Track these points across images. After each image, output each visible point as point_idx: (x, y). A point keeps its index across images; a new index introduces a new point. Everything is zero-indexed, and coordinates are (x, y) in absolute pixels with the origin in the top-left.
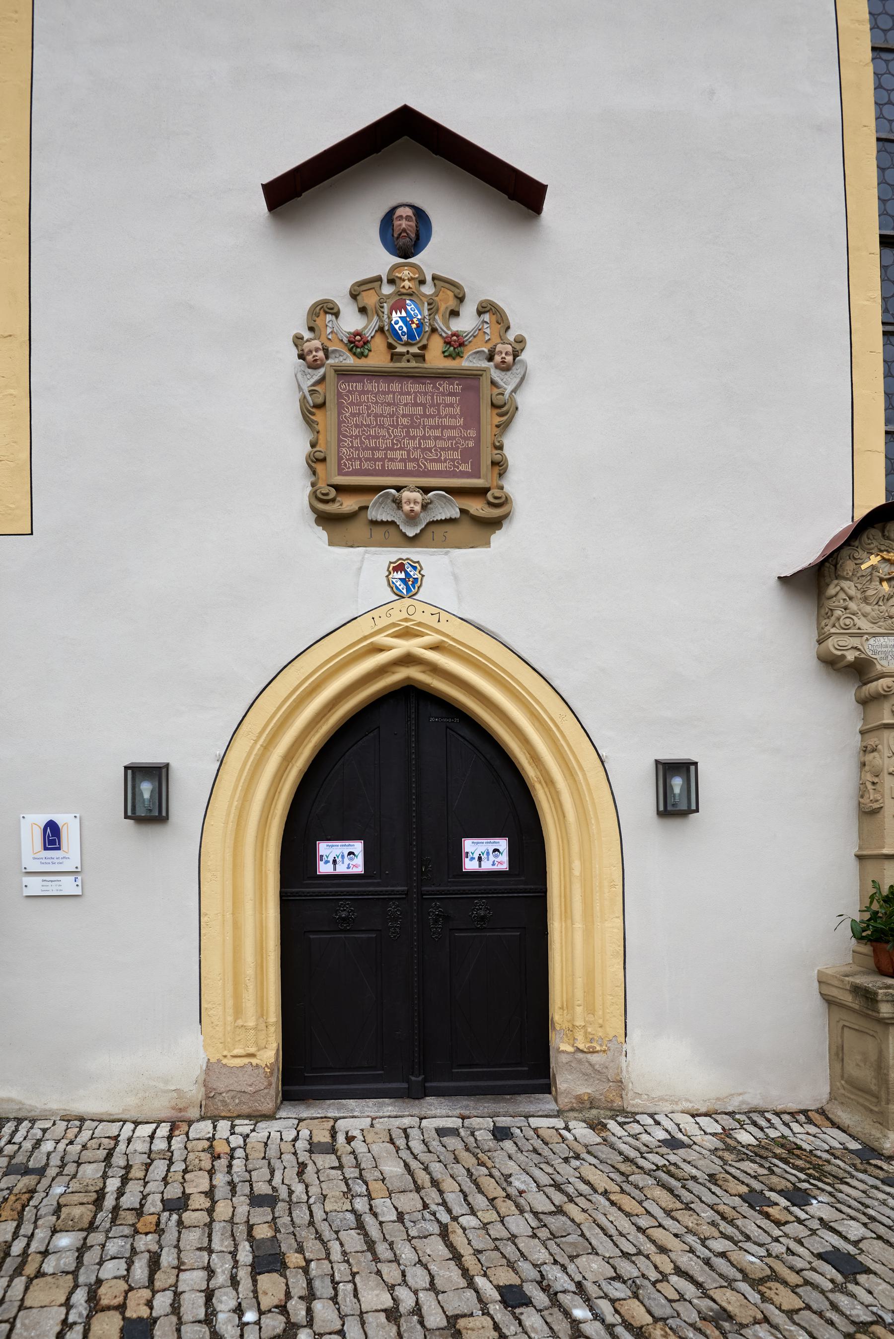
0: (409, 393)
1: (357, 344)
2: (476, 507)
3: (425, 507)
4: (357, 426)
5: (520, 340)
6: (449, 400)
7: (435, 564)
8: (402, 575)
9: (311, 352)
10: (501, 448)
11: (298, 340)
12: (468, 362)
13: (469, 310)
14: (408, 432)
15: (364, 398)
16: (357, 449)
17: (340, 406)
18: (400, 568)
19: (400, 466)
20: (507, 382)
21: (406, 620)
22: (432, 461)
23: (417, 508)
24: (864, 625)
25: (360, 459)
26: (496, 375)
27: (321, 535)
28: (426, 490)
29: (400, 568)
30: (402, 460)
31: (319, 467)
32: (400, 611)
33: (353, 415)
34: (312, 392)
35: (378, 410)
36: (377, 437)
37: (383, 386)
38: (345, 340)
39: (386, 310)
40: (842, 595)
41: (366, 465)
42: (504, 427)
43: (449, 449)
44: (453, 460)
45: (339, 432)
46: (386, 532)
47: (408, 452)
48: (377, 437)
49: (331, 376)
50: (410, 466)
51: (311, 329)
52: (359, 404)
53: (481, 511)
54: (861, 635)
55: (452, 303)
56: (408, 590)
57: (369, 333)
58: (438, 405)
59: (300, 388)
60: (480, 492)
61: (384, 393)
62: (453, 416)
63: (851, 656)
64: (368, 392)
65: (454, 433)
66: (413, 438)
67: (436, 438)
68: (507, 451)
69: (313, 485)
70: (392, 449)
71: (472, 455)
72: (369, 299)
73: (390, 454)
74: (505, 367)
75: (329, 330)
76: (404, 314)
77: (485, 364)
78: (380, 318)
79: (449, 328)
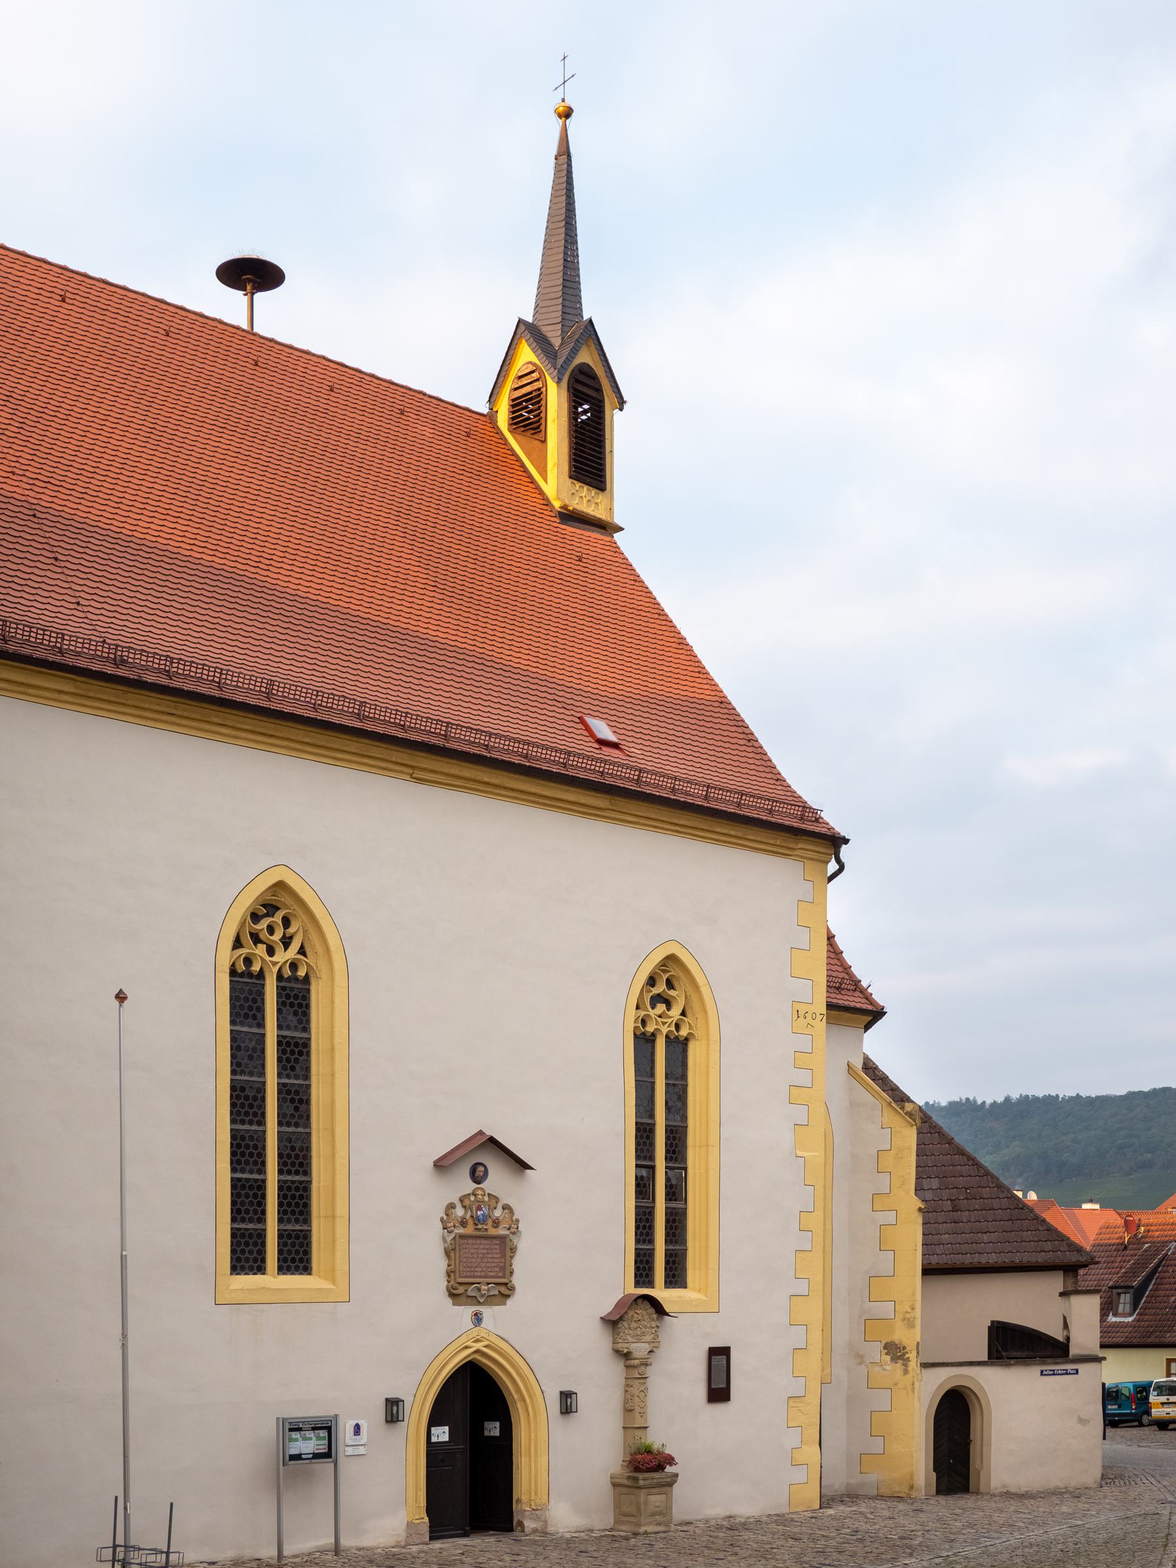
2: (503, 1289)
7: (487, 1312)
53: (504, 1292)
71: (503, 1269)
72: (467, 1202)
77: (507, 1232)
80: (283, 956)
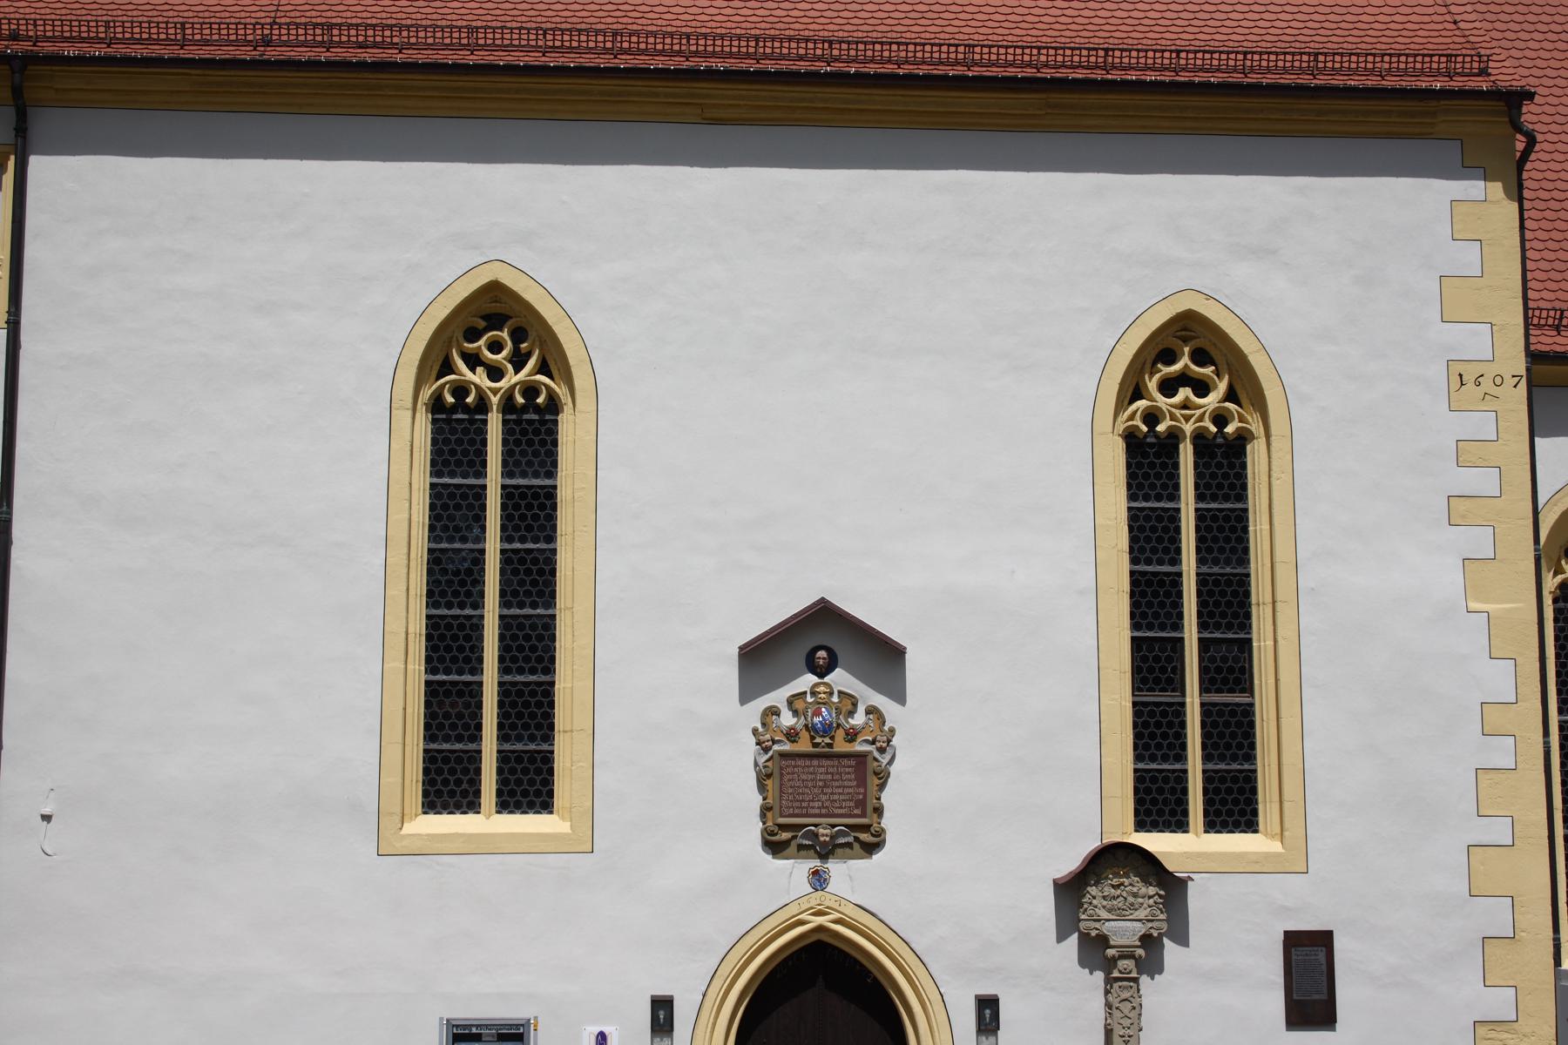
1: (792, 735)
2: (864, 837)
5: (892, 731)
7: (837, 869)
11: (755, 731)
12: (859, 747)
13: (861, 709)
18: (816, 873)
20: (884, 760)
24: (1104, 915)
26: (876, 754)
28: (833, 826)
32: (816, 899)
42: (882, 787)
49: (777, 757)
55: (850, 707)
60: (866, 828)
63: (1093, 933)
71: (862, 804)
72: (799, 705)
80: (511, 379)
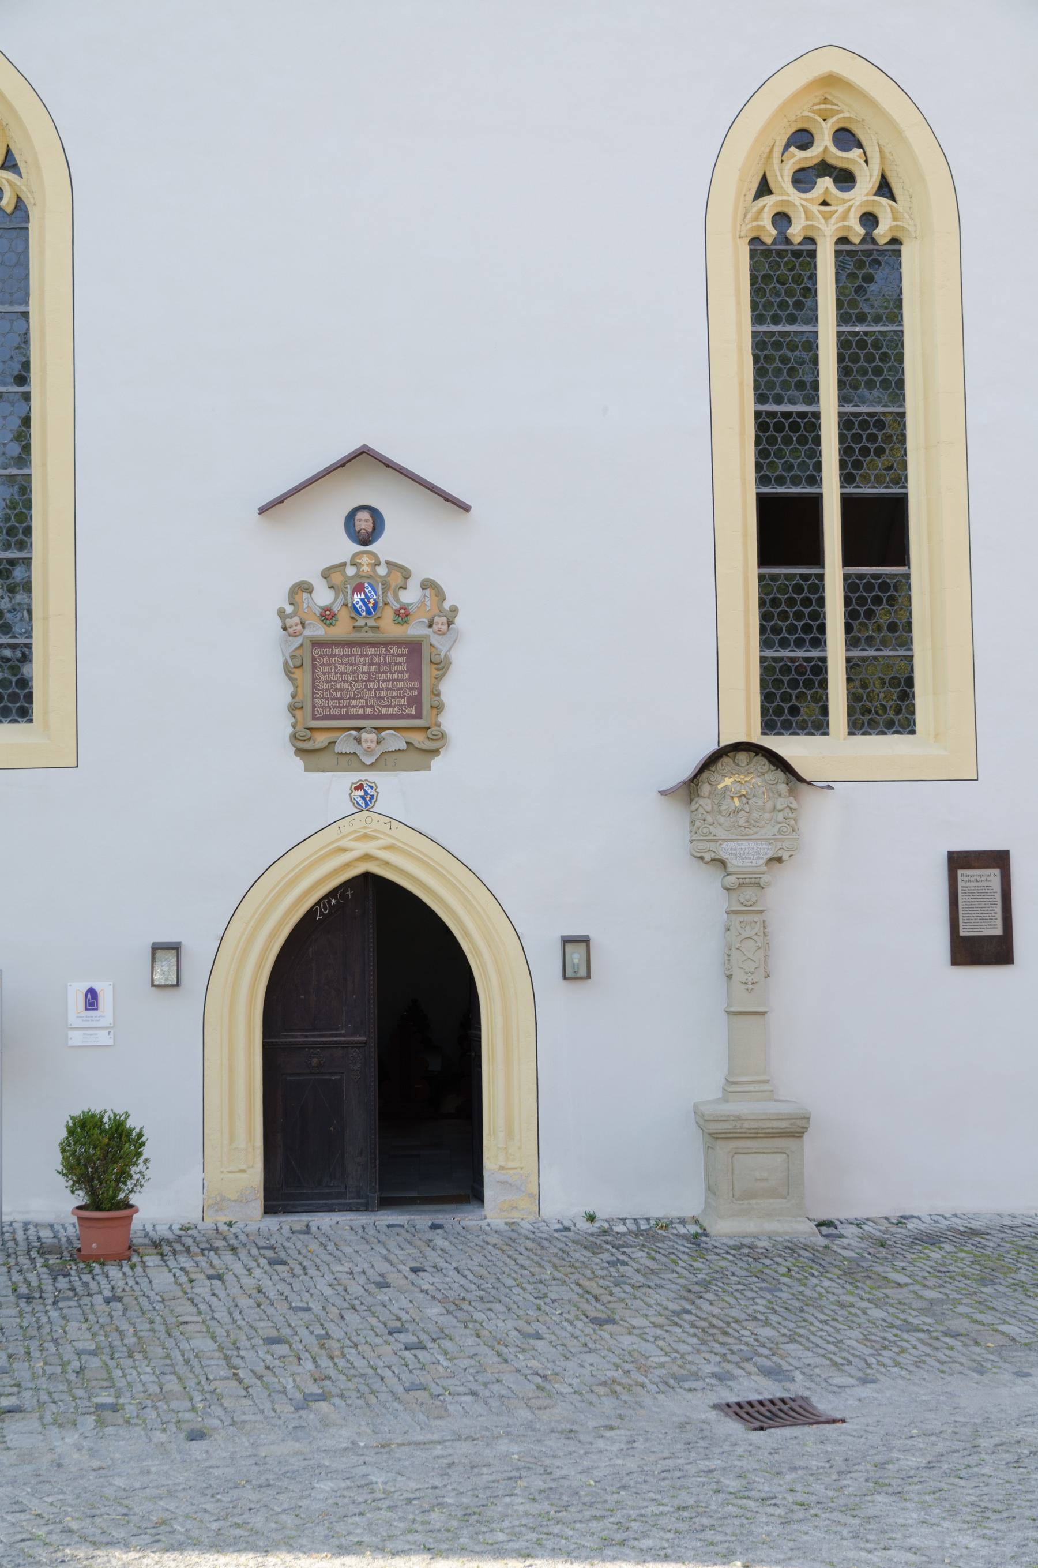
0: (367, 656)
1: (327, 616)
3: (378, 743)
4: (327, 682)
5: (454, 610)
6: (397, 659)
8: (362, 793)
9: (291, 627)
10: (438, 695)
11: (281, 613)
13: (414, 584)
14: (366, 685)
15: (332, 660)
16: (327, 699)
17: (314, 667)
18: (360, 787)
19: (360, 711)
21: (365, 828)
22: (384, 706)
23: (373, 745)
24: (720, 833)
25: (329, 707)
27: (299, 763)
28: (379, 730)
29: (360, 787)
30: (361, 707)
31: (298, 713)
33: (324, 673)
34: (293, 657)
35: (343, 669)
36: (342, 690)
37: (347, 651)
38: (318, 614)
39: (349, 591)
40: (701, 810)
41: (334, 712)
42: (439, 679)
43: (398, 697)
44: (401, 706)
45: (314, 687)
46: (351, 761)
47: (366, 700)
48: (342, 690)
50: (368, 711)
51: (291, 604)
52: (329, 665)
54: (716, 841)
55: (400, 581)
56: (367, 805)
57: (336, 608)
58: (390, 664)
59: (283, 654)
61: (348, 656)
62: (401, 672)
64: (335, 656)
65: (402, 685)
66: (370, 690)
67: (388, 689)
68: (443, 697)
69: (294, 726)
70: (354, 699)
71: (416, 701)
73: (352, 703)
74: (440, 633)
75: (305, 606)
76: (363, 596)
77: (428, 631)
78: (345, 597)
79: (397, 600)
